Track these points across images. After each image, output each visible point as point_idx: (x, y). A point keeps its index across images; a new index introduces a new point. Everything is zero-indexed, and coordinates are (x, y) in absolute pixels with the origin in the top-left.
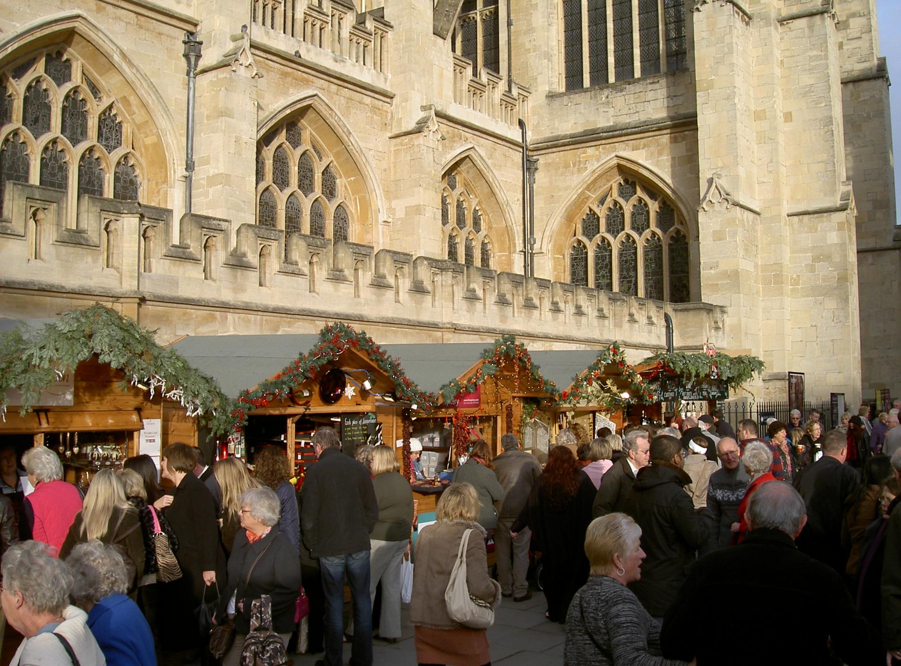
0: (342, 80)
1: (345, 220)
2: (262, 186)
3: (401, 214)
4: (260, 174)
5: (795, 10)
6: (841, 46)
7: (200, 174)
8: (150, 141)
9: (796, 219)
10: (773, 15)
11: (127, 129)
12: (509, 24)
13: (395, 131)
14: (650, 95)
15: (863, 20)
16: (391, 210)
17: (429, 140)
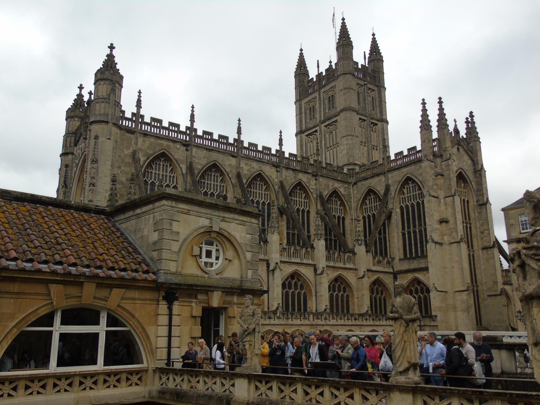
0: (346, 269)
1: (348, 297)
2: (330, 293)
3: (360, 296)
4: (329, 291)
5: (453, 241)
6: (482, 238)
7: (318, 294)
8: (309, 288)
9: (456, 293)
10: (448, 242)
11: (305, 287)
12: (389, 241)
13: (358, 277)
14: (422, 261)
15: (487, 231)
16: (358, 295)
17: (366, 279)
